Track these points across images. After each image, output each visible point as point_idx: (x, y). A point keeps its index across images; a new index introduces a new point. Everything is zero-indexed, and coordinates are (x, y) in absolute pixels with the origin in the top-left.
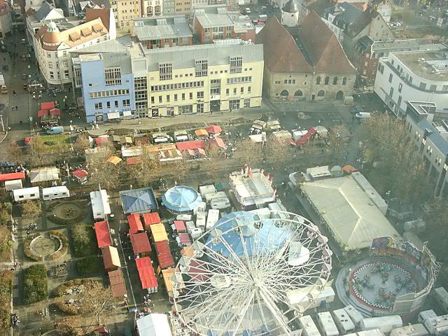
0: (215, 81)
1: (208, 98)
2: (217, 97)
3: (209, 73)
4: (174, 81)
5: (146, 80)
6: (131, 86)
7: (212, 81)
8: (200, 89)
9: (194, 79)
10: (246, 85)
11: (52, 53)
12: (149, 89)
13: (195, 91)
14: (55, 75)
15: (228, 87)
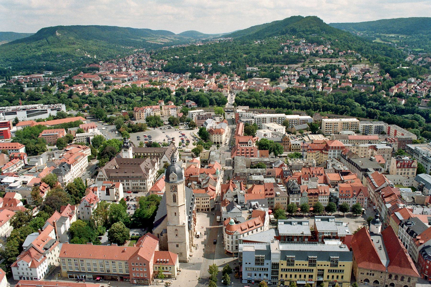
0: (320, 270)
1: (315, 278)
2: (321, 279)
3: (317, 265)
4: (295, 267)
5: (278, 265)
6: (269, 267)
7: (318, 270)
8: (311, 274)
9: (307, 267)
10: (340, 275)
11: (230, 236)
12: (280, 270)
13: (307, 274)
15: (329, 274)
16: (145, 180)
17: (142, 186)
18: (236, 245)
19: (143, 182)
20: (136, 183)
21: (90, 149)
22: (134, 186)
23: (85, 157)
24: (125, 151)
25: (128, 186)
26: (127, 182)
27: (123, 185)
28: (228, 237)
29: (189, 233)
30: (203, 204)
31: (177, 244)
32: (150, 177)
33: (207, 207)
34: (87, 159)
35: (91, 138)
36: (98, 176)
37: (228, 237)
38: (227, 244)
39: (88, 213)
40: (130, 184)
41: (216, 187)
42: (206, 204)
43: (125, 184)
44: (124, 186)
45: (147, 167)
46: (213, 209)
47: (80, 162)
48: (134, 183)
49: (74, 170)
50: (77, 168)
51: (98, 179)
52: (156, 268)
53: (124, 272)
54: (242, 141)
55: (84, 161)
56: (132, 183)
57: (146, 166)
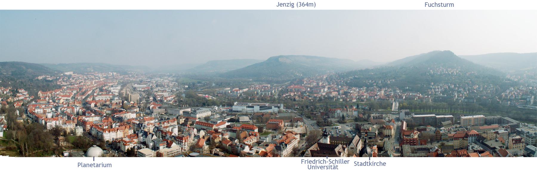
23: (296, 140)
24: (324, 138)
34: (297, 142)
36: (305, 154)
45: (340, 151)
47: (293, 143)
49: (289, 148)
50: (291, 147)
54: (407, 134)
55: (295, 143)
57: (339, 150)
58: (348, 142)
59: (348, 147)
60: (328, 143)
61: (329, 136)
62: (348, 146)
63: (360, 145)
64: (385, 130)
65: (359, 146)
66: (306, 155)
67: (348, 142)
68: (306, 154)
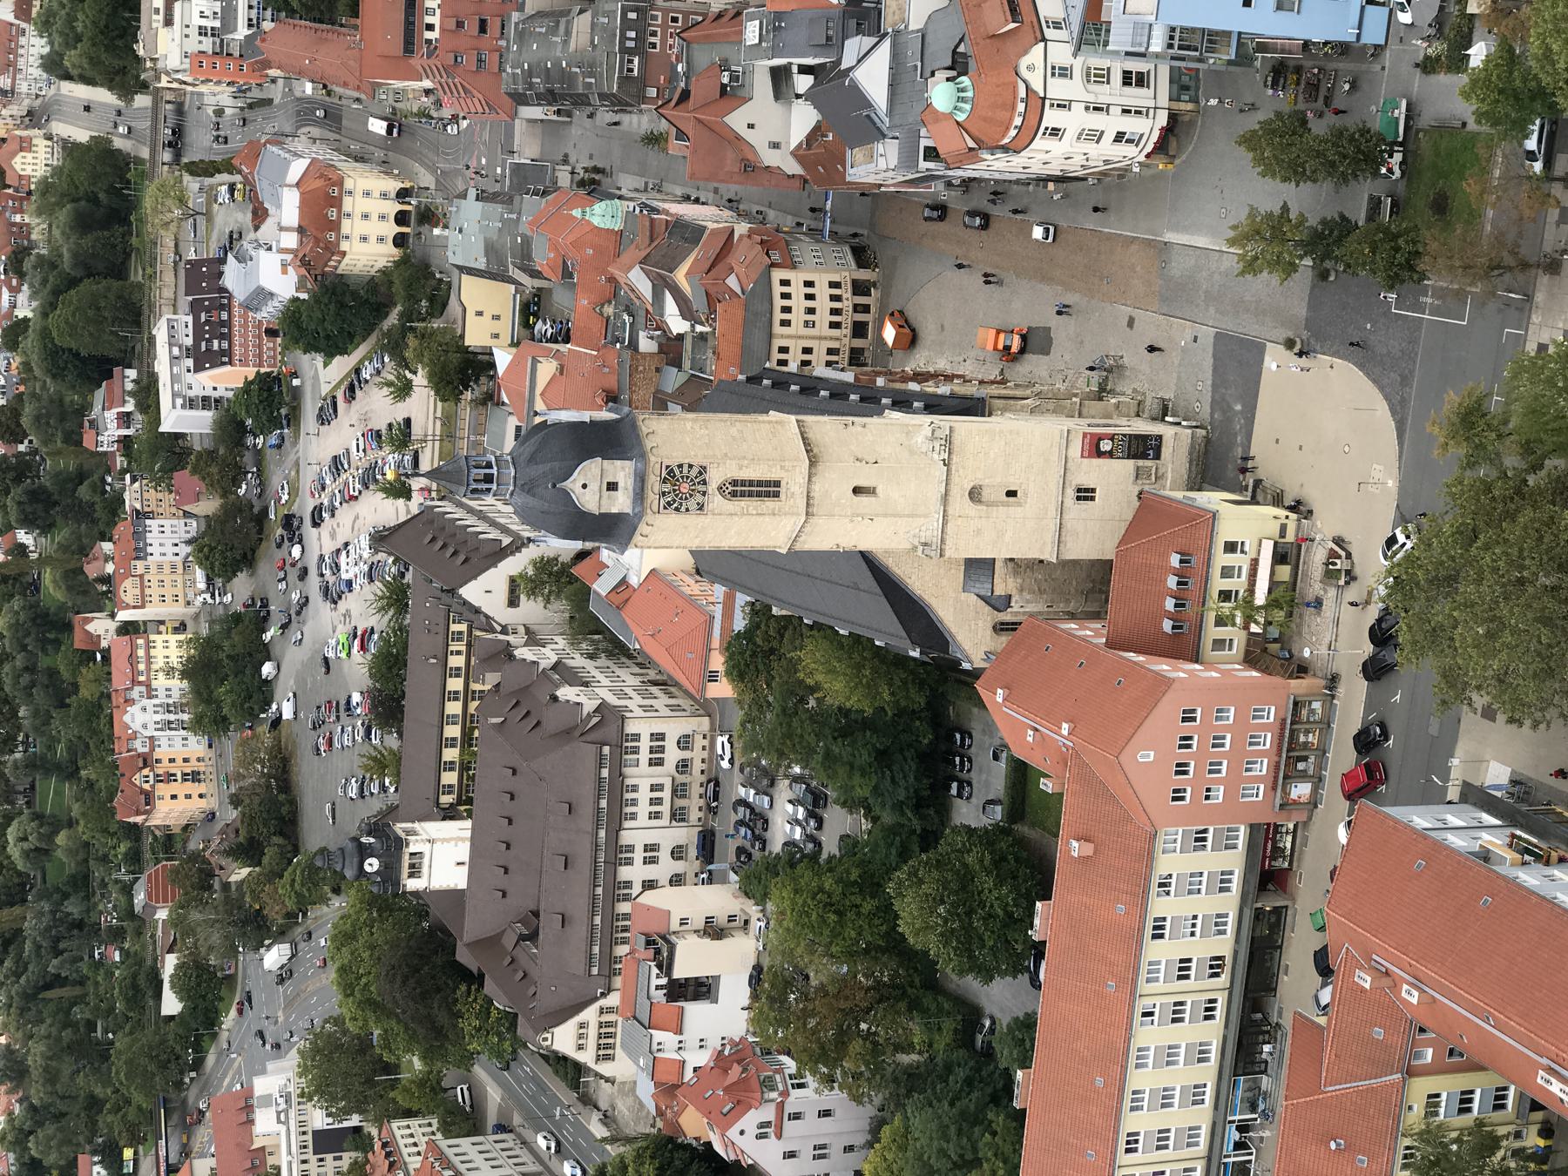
11: (1051, 118)
14: (1133, 125)
16: (631, 728)
17: (673, 755)
18: (1117, 78)
19: (645, 744)
20: (644, 795)
21: (395, 1125)
22: (665, 808)
24: (415, 871)
25: (664, 855)
26: (638, 855)
27: (649, 885)
28: (1055, 132)
29: (1004, 410)
30: (823, 317)
31: (1071, 493)
32: (613, 700)
33: (846, 292)
34: (465, 1143)
35: (319, 1119)
36: (581, 1057)
37: (1055, 132)
38: (1108, 151)
39: (826, 1113)
40: (651, 837)
41: (711, 226)
42: (823, 304)
43: (651, 872)
44: (664, 880)
46: (862, 256)
48: (643, 809)
51: (598, 1058)
52: (1219, 644)
53: (1234, 861)
56: (643, 820)
58: (454, 627)
59: (504, 631)
60: (468, 834)
61: (399, 828)
62: (493, 631)
63: (481, 516)
64: (344, 246)
65: (494, 524)
66: (592, 1042)
67: (454, 627)
68: (580, 1048)
